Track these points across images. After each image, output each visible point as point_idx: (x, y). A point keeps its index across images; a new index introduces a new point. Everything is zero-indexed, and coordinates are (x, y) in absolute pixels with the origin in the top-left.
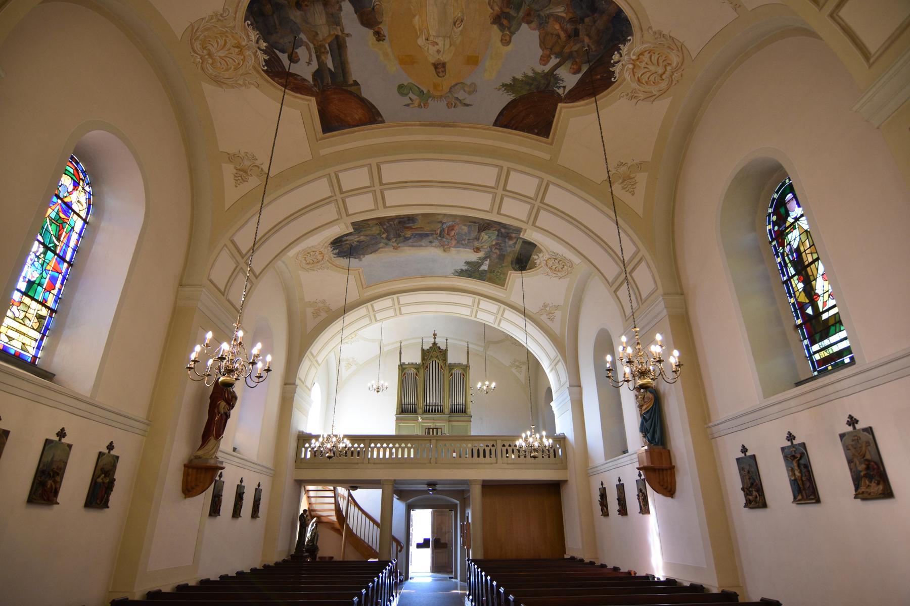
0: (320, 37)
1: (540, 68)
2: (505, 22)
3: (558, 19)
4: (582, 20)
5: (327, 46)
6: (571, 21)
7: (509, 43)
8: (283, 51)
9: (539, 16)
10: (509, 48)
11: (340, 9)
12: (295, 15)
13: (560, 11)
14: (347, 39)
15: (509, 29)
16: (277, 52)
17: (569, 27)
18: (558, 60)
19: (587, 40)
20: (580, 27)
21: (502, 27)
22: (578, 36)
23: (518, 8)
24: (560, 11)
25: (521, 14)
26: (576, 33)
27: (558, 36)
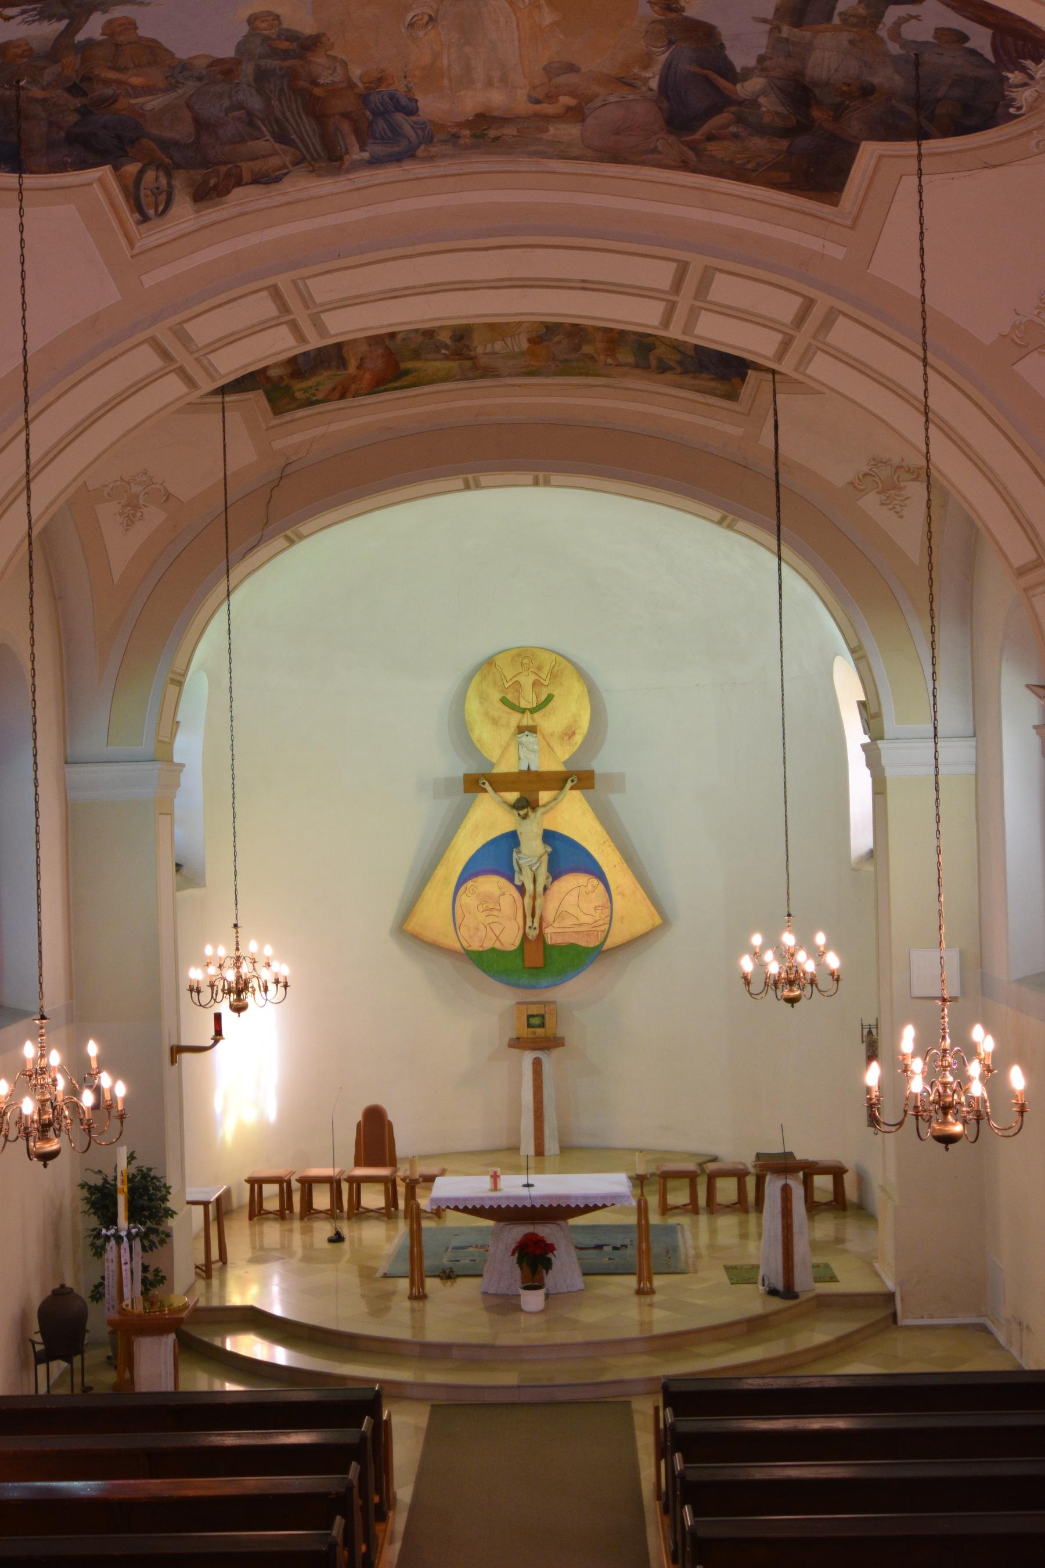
0: (845, 36)
1: (119, 12)
2: (285, 45)
3: (149, 90)
4: (84, 112)
5: (836, 20)
6: (114, 99)
7: (252, 20)
8: (973, 52)
9: (200, 79)
10: (249, 12)
11: (761, 59)
12: (885, 77)
13: (152, 103)
14: (770, 14)
15: (266, 39)
16: (990, 57)
17: (101, 91)
18: (80, 37)
19: (37, 92)
20: (78, 102)
21: (291, 36)
22: (69, 90)
23: (261, 76)
24: (152, 103)
25: (248, 69)
26: (75, 90)
27: (118, 70)
